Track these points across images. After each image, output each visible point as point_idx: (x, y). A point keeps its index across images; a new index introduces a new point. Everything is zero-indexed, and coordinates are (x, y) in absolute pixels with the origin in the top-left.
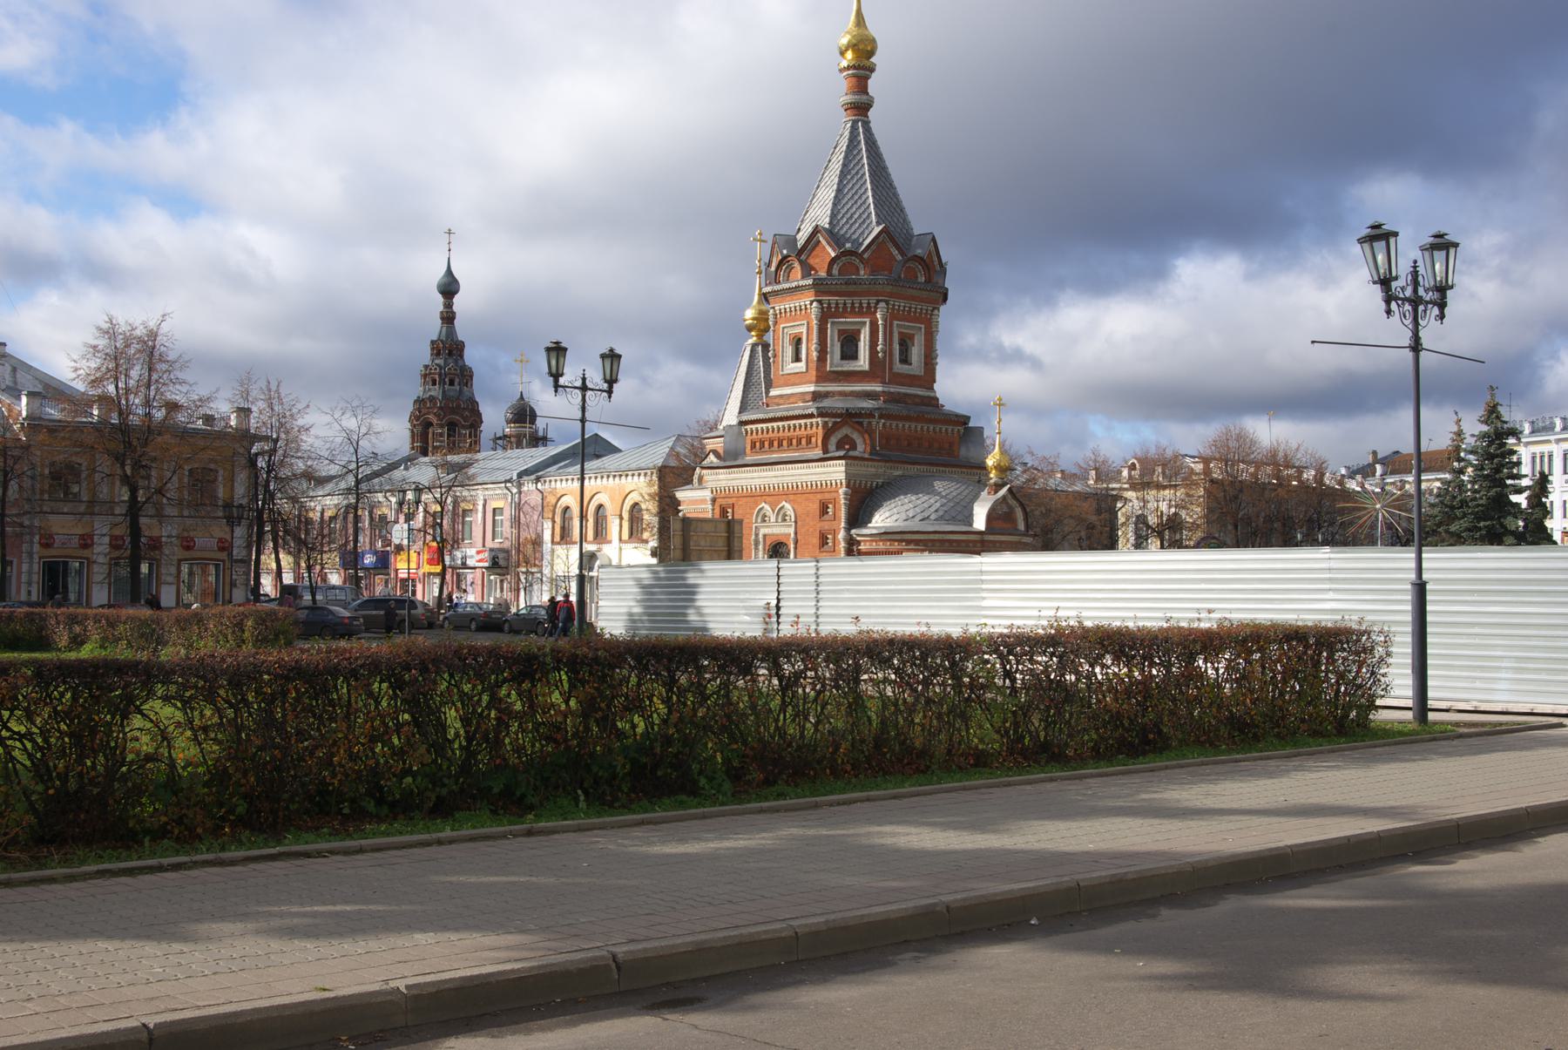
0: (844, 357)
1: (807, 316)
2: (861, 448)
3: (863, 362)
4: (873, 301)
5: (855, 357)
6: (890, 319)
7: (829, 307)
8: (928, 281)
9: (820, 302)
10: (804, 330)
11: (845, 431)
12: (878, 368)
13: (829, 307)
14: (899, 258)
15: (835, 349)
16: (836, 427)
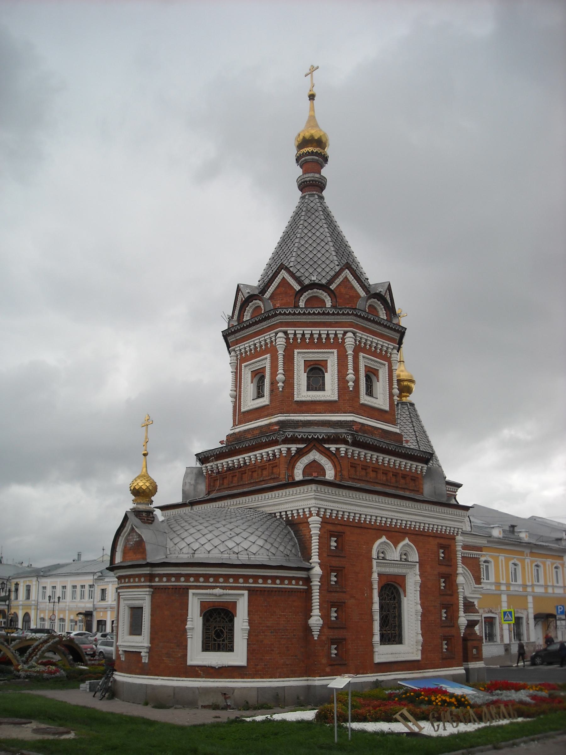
0: (310, 388)
1: (273, 350)
2: (330, 474)
3: (330, 392)
4: (340, 331)
5: (322, 388)
6: (358, 349)
7: (295, 338)
8: (390, 320)
9: (285, 333)
10: (266, 362)
11: (314, 455)
12: (348, 399)
13: (295, 338)
14: (362, 293)
15: (301, 377)
16: (300, 453)
